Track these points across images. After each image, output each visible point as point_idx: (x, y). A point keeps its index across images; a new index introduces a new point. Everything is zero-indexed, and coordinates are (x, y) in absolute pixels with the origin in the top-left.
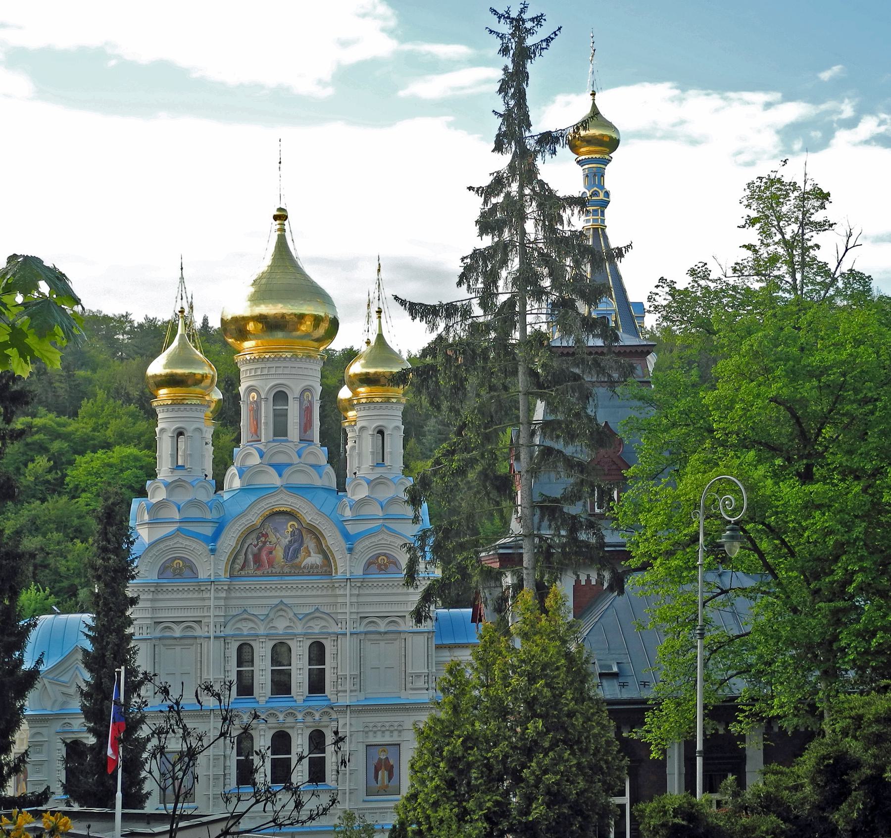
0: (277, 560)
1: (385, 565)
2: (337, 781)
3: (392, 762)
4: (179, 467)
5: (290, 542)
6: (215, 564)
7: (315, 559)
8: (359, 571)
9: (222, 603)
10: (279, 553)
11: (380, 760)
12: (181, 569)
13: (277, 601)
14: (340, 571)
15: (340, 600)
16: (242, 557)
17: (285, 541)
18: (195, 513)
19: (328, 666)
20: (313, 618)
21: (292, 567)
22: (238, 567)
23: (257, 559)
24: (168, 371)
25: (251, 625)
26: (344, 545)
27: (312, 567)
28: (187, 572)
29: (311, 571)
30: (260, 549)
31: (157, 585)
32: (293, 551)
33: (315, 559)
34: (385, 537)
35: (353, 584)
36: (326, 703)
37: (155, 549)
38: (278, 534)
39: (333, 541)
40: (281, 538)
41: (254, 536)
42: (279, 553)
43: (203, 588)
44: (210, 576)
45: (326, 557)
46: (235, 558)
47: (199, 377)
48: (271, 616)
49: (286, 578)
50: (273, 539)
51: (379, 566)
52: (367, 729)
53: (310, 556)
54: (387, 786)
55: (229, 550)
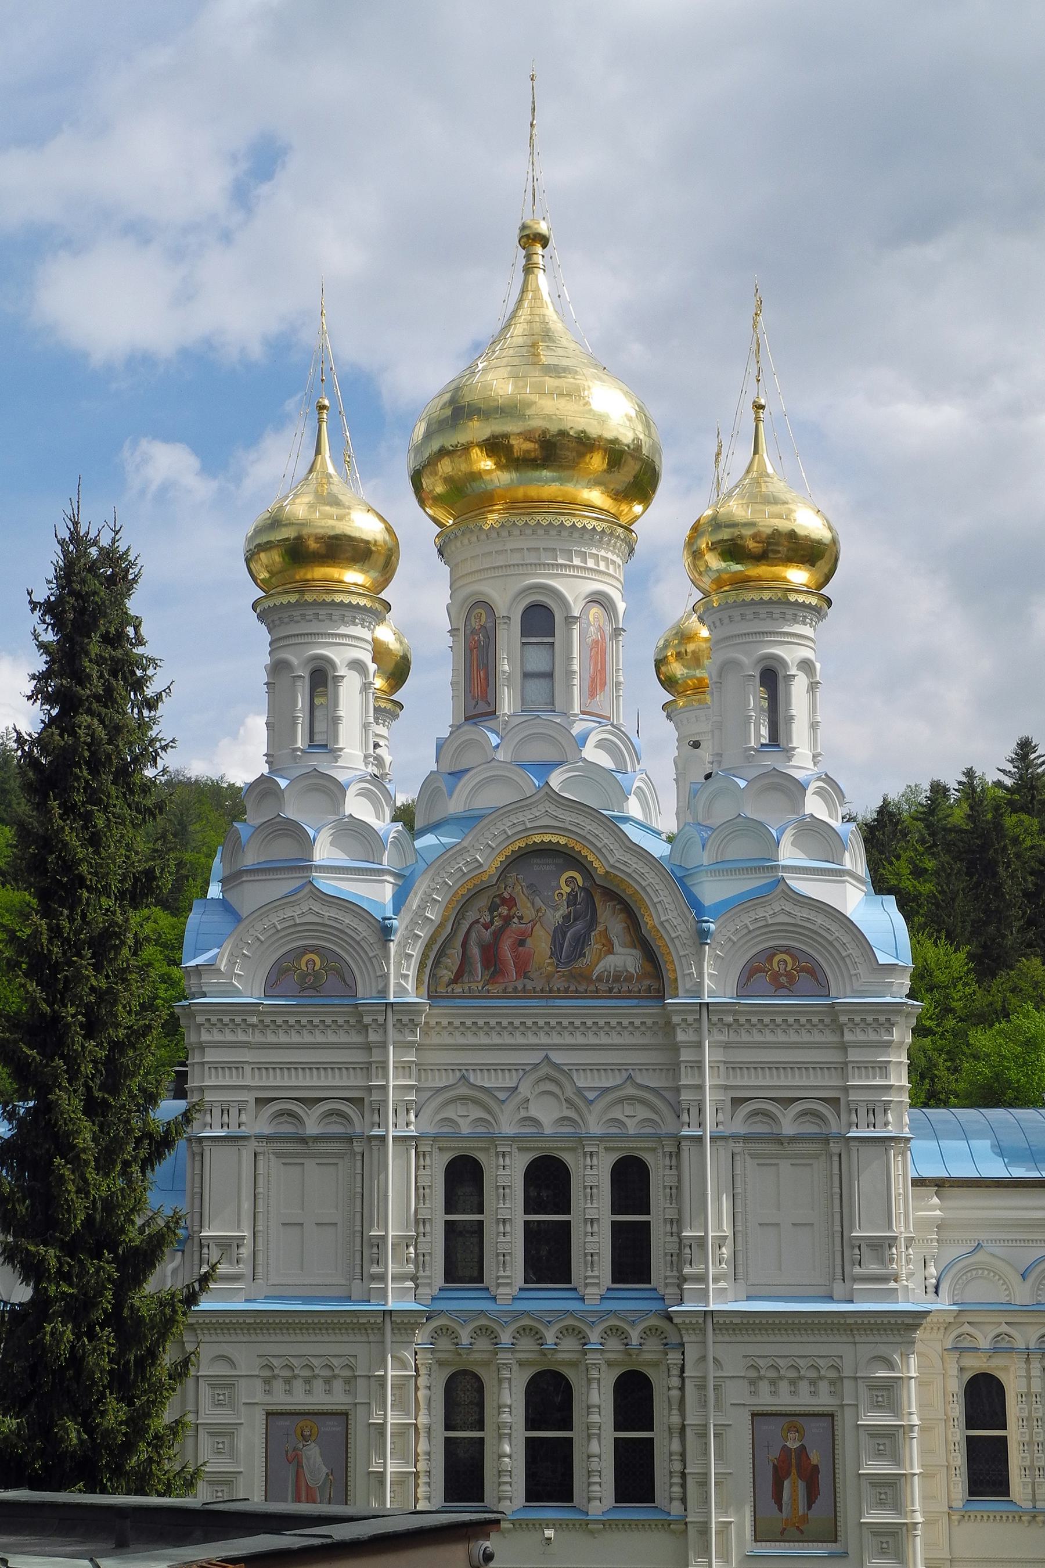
1: (788, 975)
2: (684, 1500)
3: (815, 1458)
5: (566, 918)
7: (624, 959)
10: (541, 944)
11: (785, 1449)
12: (316, 975)
13: (535, 1057)
17: (555, 917)
19: (658, 1216)
20: (621, 1101)
22: (446, 975)
23: (491, 956)
25: (478, 1113)
27: (617, 979)
29: (615, 987)
30: (498, 935)
36: (654, 1306)
38: (537, 900)
39: (665, 915)
46: (441, 953)
48: (525, 1090)
50: (525, 909)
51: (776, 976)
52: (753, 1374)
53: (611, 951)
54: (805, 1519)
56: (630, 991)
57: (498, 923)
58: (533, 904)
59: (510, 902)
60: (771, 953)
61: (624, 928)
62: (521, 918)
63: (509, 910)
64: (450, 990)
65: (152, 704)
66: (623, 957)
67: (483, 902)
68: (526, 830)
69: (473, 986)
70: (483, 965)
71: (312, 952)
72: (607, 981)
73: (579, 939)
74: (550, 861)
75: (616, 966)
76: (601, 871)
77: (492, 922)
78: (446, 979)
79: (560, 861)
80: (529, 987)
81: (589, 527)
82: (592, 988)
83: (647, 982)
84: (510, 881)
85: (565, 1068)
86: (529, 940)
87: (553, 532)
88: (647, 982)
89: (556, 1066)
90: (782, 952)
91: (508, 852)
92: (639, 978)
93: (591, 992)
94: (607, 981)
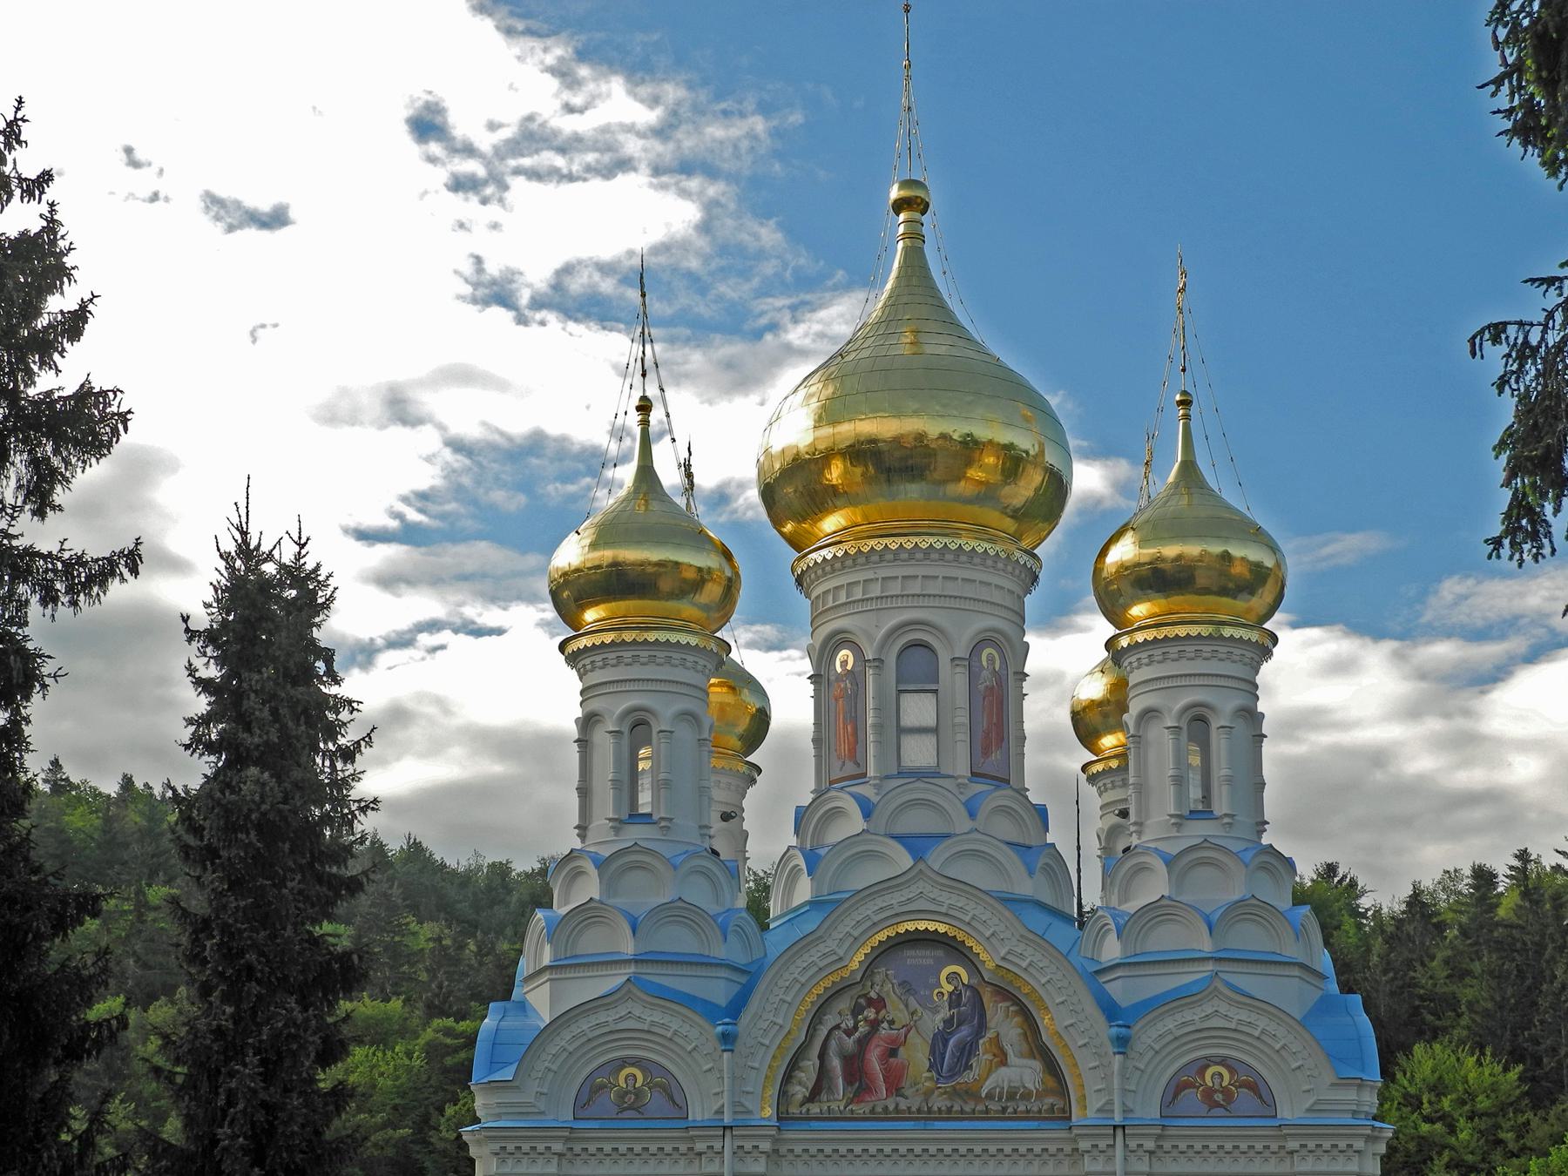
4: (635, 817)
5: (948, 1022)
6: (733, 1078)
10: (917, 1055)
12: (638, 1093)
14: (1095, 1103)
16: (811, 1064)
17: (934, 1022)
18: (678, 940)
21: (955, 1093)
22: (799, 1091)
23: (855, 1068)
24: (607, 555)
26: (1105, 1031)
27: (1012, 1096)
28: (655, 1102)
30: (863, 1043)
31: (571, 1135)
32: (956, 1051)
35: (1133, 1144)
37: (567, 1035)
39: (1069, 1018)
41: (845, 1004)
42: (917, 1055)
43: (700, 1146)
44: (720, 1112)
45: (1052, 1067)
46: (793, 1066)
47: (690, 575)
49: (938, 1125)
50: (896, 1010)
56: (1028, 1111)
57: (863, 1028)
58: (907, 1006)
59: (879, 1003)
62: (891, 1022)
63: (877, 1013)
65: (349, 755)
69: (834, 1106)
70: (845, 1079)
71: (633, 1065)
72: (1000, 1099)
76: (990, 965)
77: (856, 1028)
78: (799, 1097)
79: (940, 953)
80: (903, 1106)
81: (980, 550)
82: (980, 1107)
83: (1050, 1100)
84: (878, 979)
86: (902, 1050)
87: (934, 556)
91: (875, 942)
92: (1040, 1096)
94: (1000, 1099)
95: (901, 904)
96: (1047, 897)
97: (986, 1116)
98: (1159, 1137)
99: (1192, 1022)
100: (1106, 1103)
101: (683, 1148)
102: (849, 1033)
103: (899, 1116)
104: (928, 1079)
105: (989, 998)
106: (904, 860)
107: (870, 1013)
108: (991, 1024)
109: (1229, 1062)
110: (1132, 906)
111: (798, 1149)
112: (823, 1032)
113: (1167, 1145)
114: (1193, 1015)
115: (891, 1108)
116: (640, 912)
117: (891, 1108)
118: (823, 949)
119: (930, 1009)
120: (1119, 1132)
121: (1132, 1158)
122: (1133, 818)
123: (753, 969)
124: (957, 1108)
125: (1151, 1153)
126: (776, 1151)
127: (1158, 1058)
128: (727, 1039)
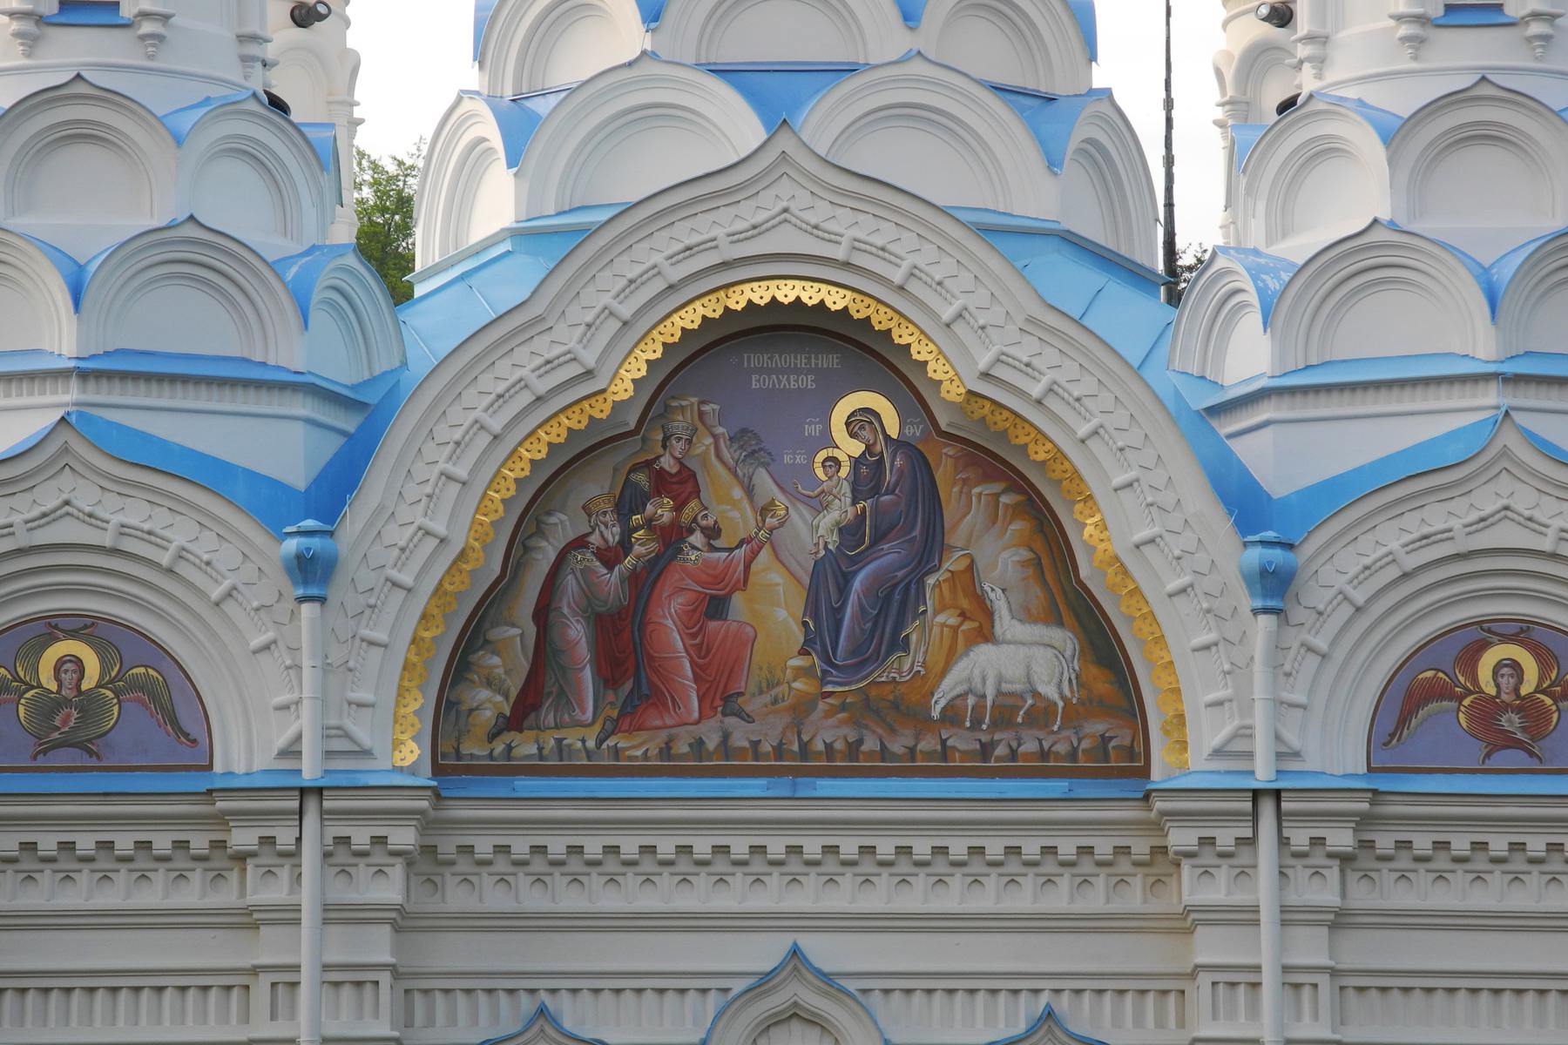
0: (760, 654)
1: (1528, 708)
5: (850, 532)
6: (326, 668)
7: (1024, 657)
8: (1338, 750)
9: (377, 946)
10: (774, 612)
12: (88, 704)
14: (1207, 733)
15: (1211, 947)
17: (814, 530)
18: (190, 324)
21: (867, 709)
22: (487, 703)
26: (1231, 556)
28: (130, 727)
29: (1001, 741)
30: (644, 583)
33: (1024, 657)
34: (1524, 499)
35: (1300, 837)
38: (763, 479)
40: (784, 513)
41: (597, 485)
42: (774, 612)
43: (243, 838)
44: (291, 752)
45: (1102, 646)
46: (473, 638)
49: (826, 786)
50: (727, 504)
53: (985, 634)
55: (422, 573)
56: (1044, 755)
57: (644, 545)
58: (749, 491)
59: (682, 485)
60: (1472, 641)
61: (1024, 564)
62: (712, 533)
63: (678, 508)
64: (499, 747)
66: (1023, 651)
67: (597, 485)
68: (726, 265)
69: (572, 738)
70: (598, 672)
71: (73, 634)
72: (976, 724)
73: (889, 597)
74: (801, 361)
75: (1000, 679)
76: (953, 392)
77: (625, 545)
78: (488, 715)
79: (830, 361)
80: (739, 740)
82: (927, 744)
83: (1097, 727)
84: (680, 423)
85: (852, 985)
86: (738, 599)
88: (1097, 727)
89: (828, 980)
90: (1507, 639)
91: (672, 331)
92: (1074, 715)
93: (929, 755)
94: (976, 724)
95: (736, 237)
96: (1093, 229)
97: (943, 765)
98: (1364, 821)
99: (1446, 535)
100: (1235, 736)
101: (200, 842)
102: (609, 557)
103: (728, 762)
104: (800, 672)
105: (962, 482)
106: (738, 127)
107: (662, 510)
108: (956, 538)
109: (1537, 634)
110: (1299, 247)
111: (484, 845)
112: (546, 554)
113: (1385, 841)
114: (1449, 517)
115: (711, 744)
116: (91, 250)
117: (711, 744)
118: (545, 347)
119: (807, 501)
120: (1267, 808)
121: (1299, 873)
122: (1304, 20)
123: (371, 397)
124: (871, 744)
125: (1345, 859)
126: (429, 850)
127: (1364, 622)
128: (312, 573)
